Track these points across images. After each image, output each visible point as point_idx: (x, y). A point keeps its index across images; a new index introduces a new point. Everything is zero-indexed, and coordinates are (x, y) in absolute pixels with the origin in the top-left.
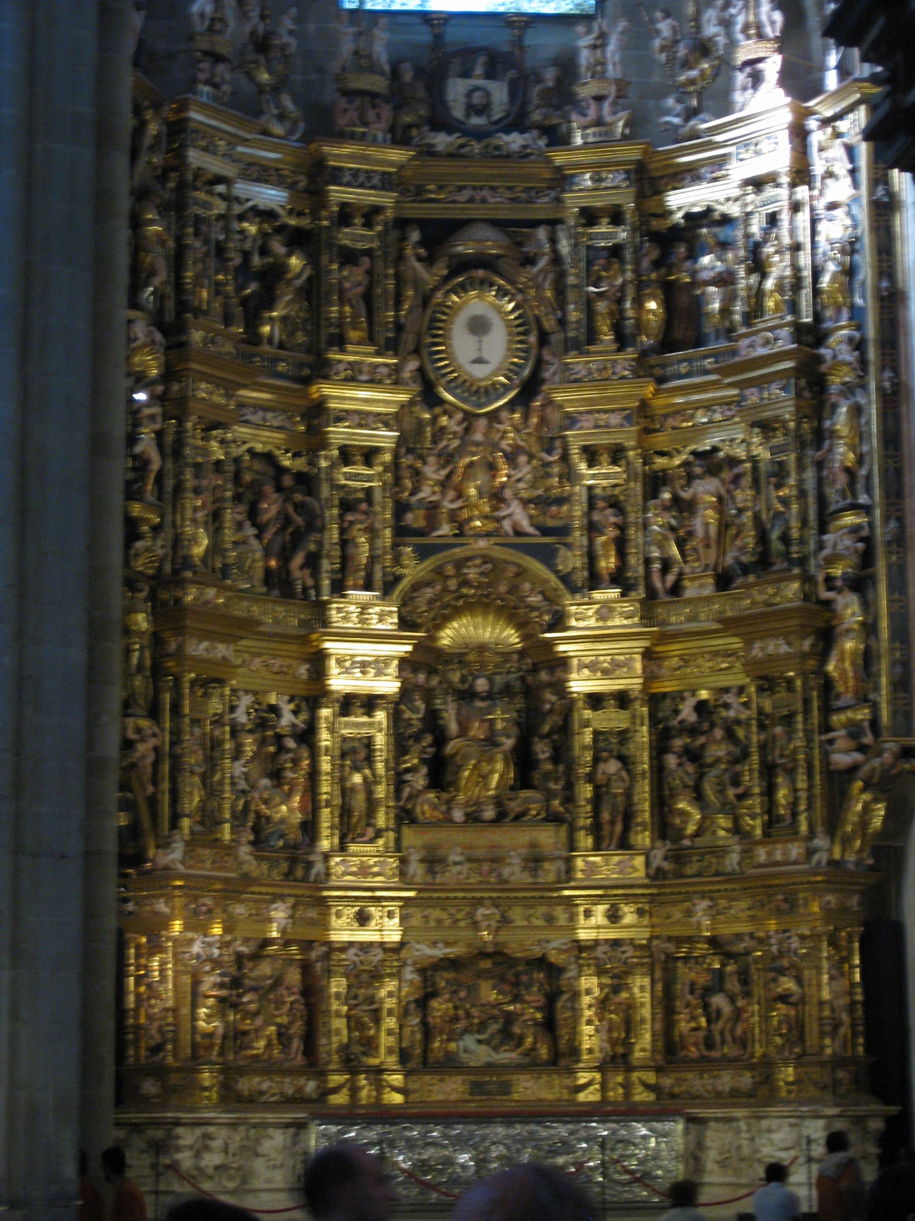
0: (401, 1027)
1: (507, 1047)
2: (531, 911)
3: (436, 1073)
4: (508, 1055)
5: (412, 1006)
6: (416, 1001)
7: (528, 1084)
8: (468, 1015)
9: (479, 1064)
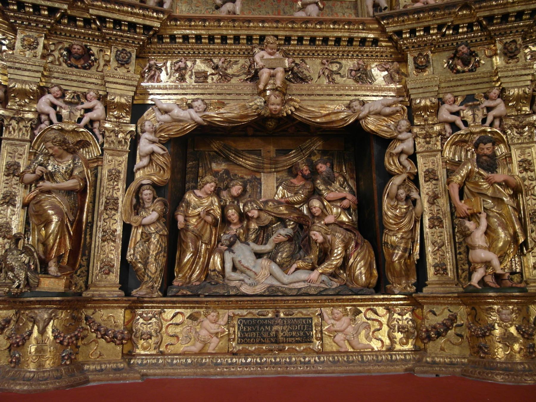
0: (127, 228)
1: (300, 264)
2: (335, 68)
3: (185, 304)
4: (303, 275)
5: (147, 193)
6: (154, 186)
7: (338, 326)
8: (243, 217)
9: (259, 289)
